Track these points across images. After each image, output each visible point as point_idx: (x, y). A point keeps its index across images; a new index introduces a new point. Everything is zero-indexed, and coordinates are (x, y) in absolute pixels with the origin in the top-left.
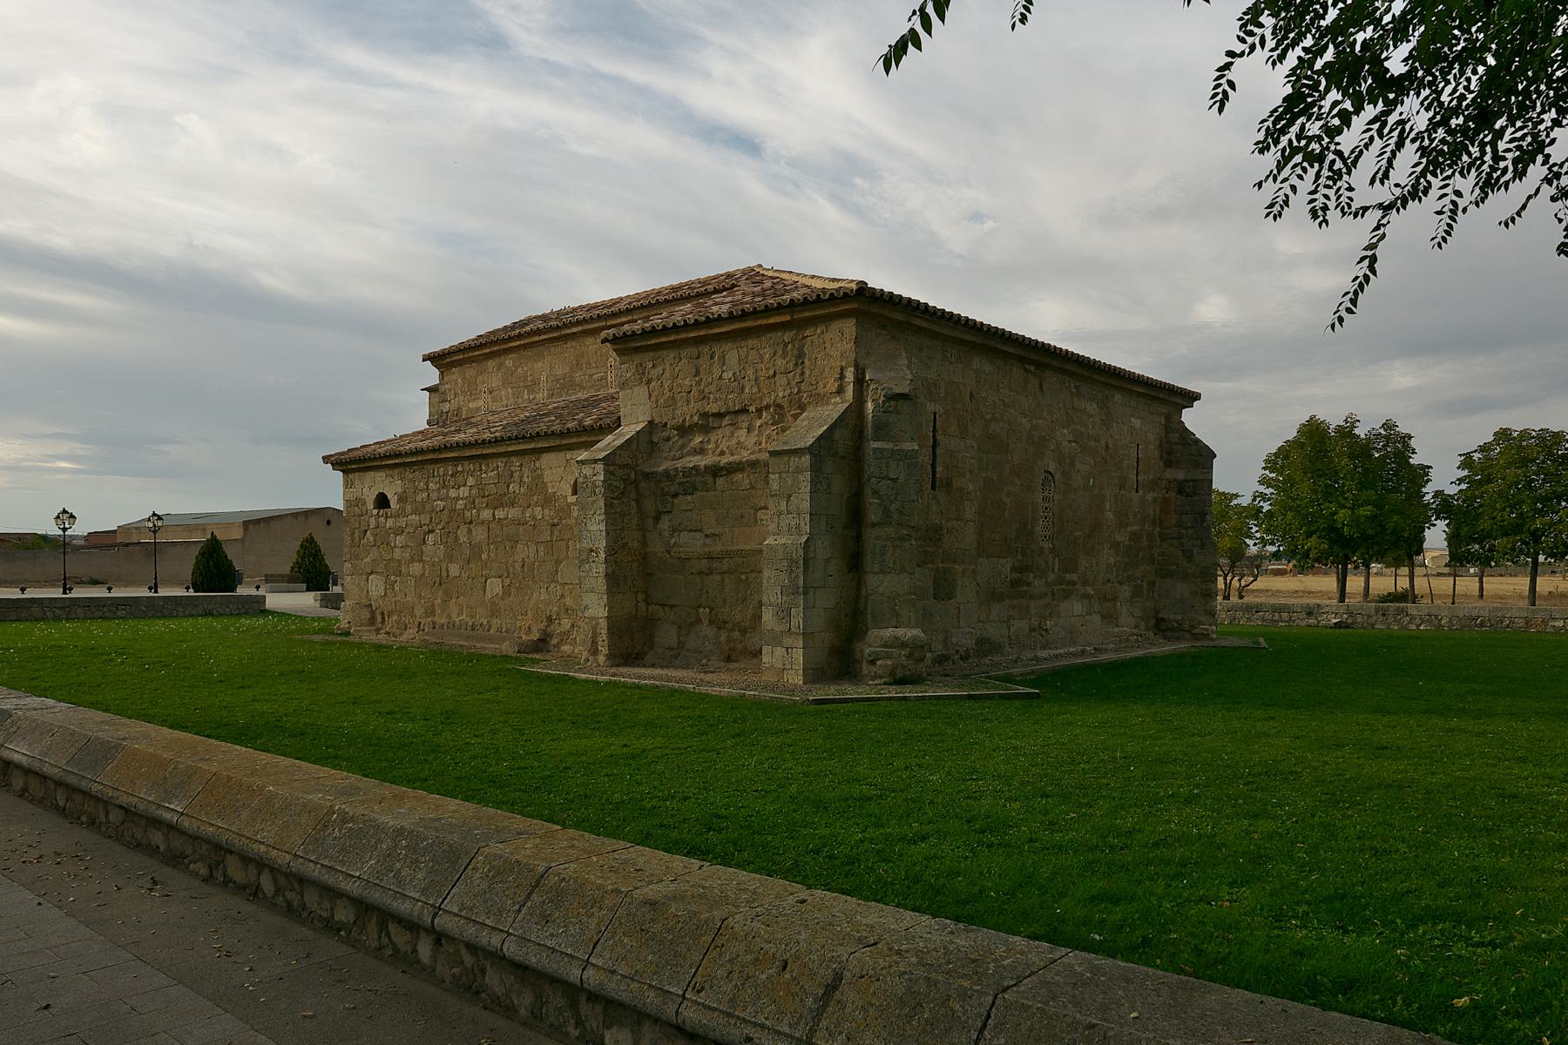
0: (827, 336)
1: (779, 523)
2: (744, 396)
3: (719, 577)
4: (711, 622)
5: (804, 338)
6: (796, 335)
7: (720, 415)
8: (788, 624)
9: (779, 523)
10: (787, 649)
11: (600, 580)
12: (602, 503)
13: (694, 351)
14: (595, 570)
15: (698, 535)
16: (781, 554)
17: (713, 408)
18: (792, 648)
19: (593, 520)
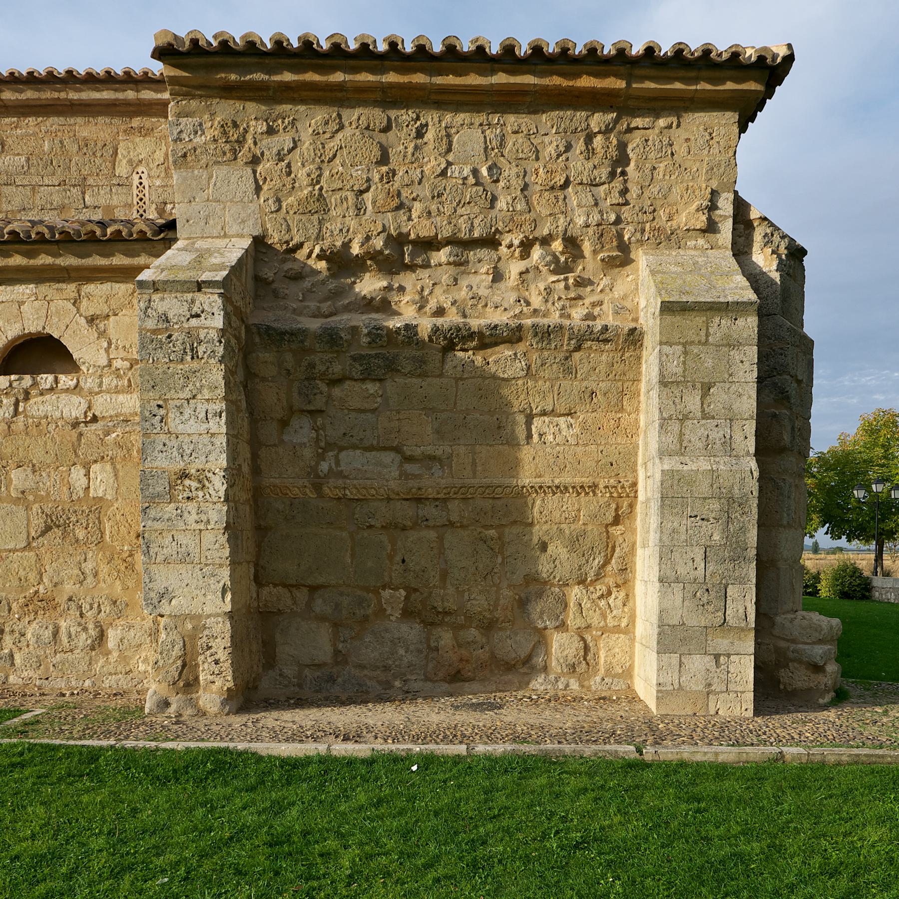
0: (680, 136)
1: (681, 434)
2: (493, 213)
3: (432, 534)
4: (408, 613)
5: (629, 130)
6: (616, 121)
7: (430, 244)
8: (720, 614)
9: (681, 434)
10: (717, 657)
11: (208, 538)
12: (216, 375)
13: (377, 116)
14: (194, 517)
15: (388, 457)
16: (704, 488)
17: (421, 228)
18: (729, 656)
19: (188, 411)
